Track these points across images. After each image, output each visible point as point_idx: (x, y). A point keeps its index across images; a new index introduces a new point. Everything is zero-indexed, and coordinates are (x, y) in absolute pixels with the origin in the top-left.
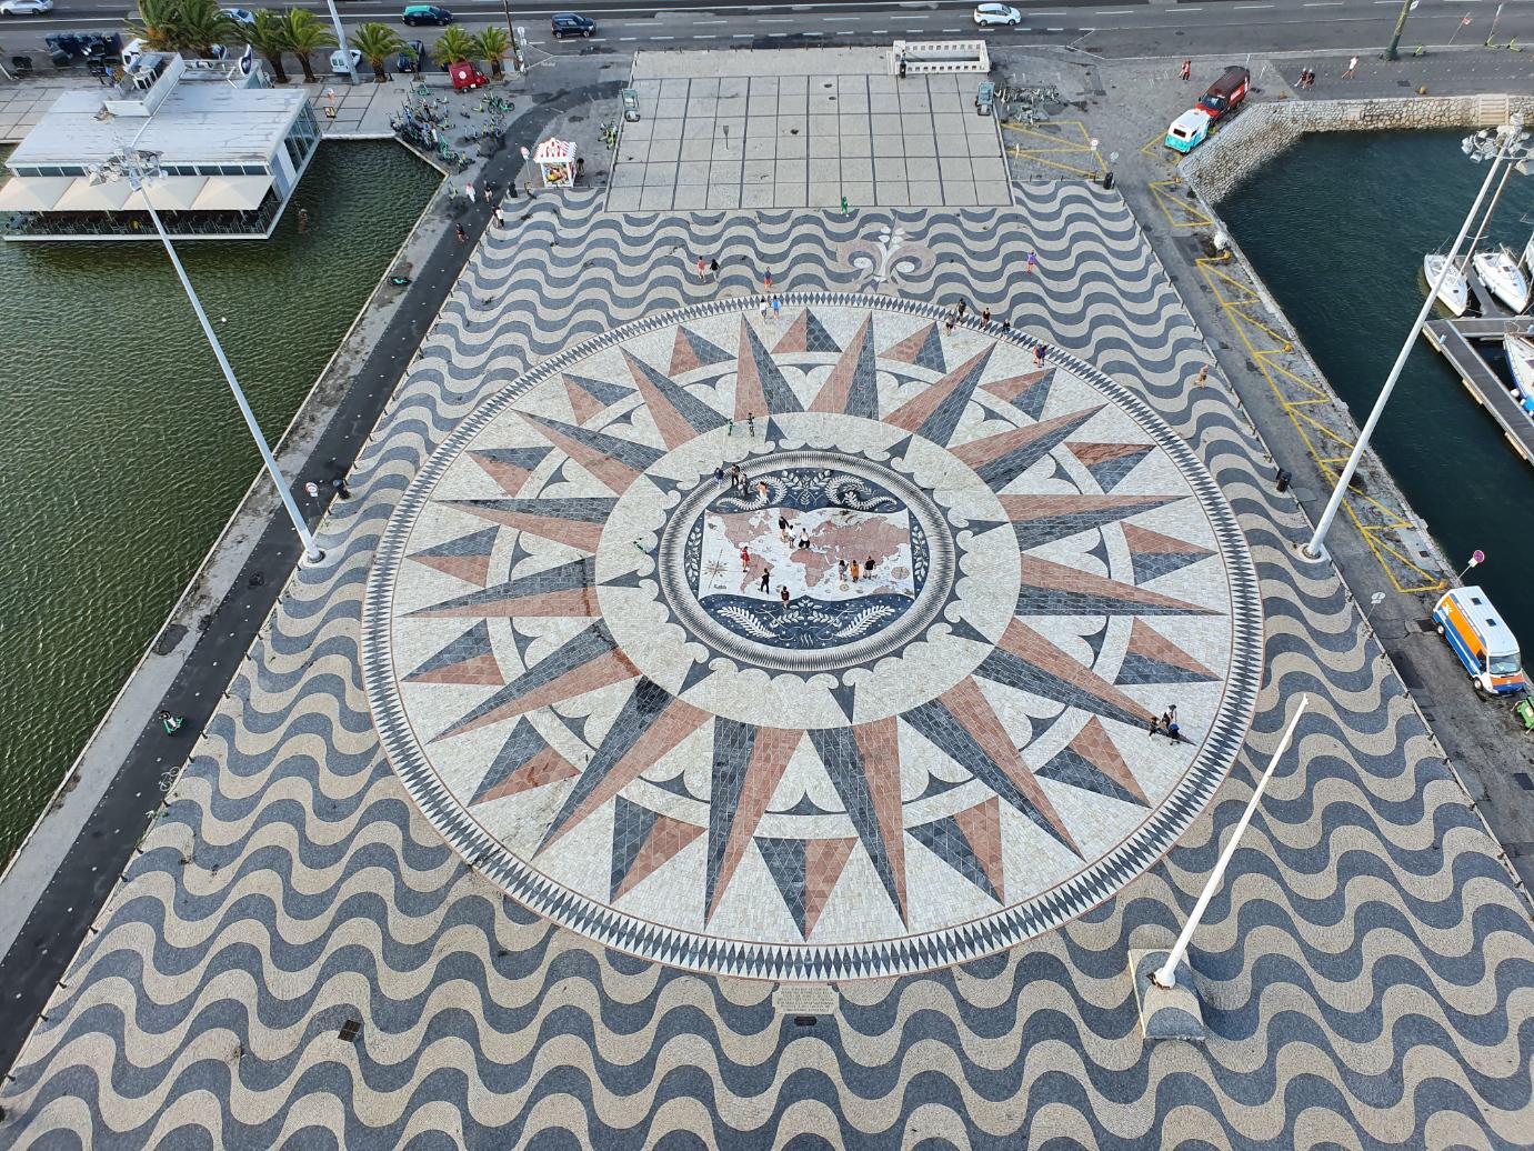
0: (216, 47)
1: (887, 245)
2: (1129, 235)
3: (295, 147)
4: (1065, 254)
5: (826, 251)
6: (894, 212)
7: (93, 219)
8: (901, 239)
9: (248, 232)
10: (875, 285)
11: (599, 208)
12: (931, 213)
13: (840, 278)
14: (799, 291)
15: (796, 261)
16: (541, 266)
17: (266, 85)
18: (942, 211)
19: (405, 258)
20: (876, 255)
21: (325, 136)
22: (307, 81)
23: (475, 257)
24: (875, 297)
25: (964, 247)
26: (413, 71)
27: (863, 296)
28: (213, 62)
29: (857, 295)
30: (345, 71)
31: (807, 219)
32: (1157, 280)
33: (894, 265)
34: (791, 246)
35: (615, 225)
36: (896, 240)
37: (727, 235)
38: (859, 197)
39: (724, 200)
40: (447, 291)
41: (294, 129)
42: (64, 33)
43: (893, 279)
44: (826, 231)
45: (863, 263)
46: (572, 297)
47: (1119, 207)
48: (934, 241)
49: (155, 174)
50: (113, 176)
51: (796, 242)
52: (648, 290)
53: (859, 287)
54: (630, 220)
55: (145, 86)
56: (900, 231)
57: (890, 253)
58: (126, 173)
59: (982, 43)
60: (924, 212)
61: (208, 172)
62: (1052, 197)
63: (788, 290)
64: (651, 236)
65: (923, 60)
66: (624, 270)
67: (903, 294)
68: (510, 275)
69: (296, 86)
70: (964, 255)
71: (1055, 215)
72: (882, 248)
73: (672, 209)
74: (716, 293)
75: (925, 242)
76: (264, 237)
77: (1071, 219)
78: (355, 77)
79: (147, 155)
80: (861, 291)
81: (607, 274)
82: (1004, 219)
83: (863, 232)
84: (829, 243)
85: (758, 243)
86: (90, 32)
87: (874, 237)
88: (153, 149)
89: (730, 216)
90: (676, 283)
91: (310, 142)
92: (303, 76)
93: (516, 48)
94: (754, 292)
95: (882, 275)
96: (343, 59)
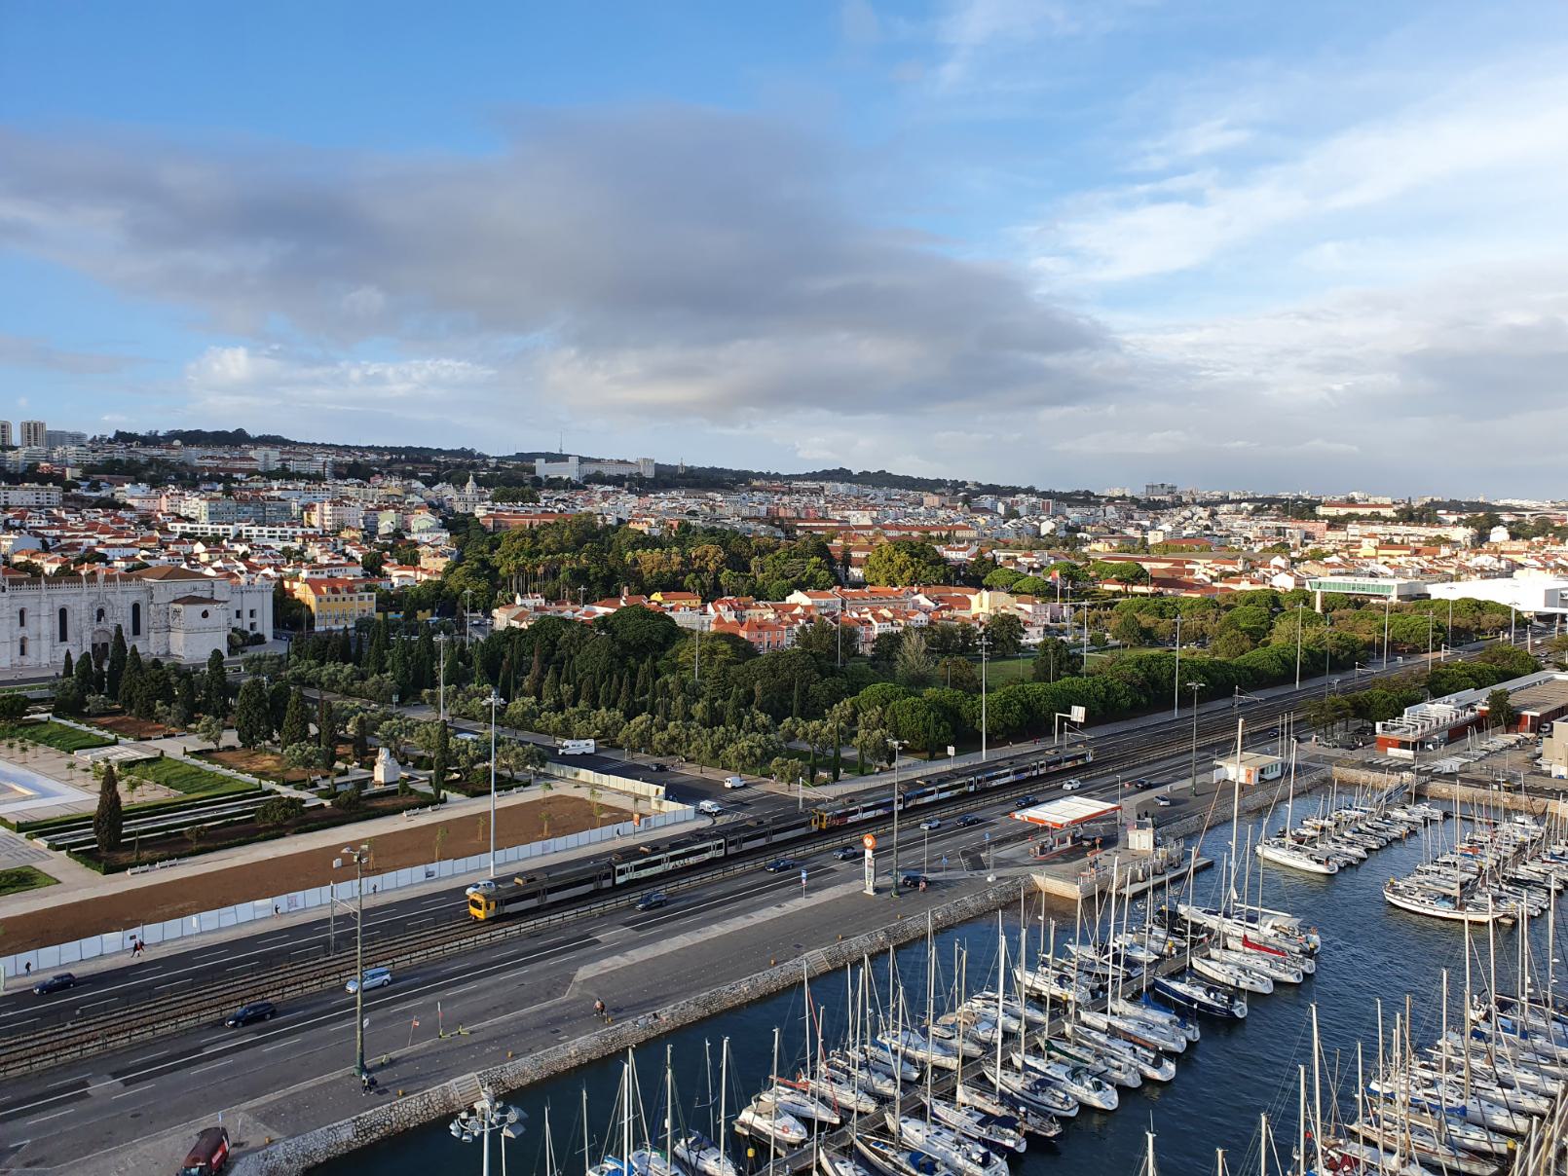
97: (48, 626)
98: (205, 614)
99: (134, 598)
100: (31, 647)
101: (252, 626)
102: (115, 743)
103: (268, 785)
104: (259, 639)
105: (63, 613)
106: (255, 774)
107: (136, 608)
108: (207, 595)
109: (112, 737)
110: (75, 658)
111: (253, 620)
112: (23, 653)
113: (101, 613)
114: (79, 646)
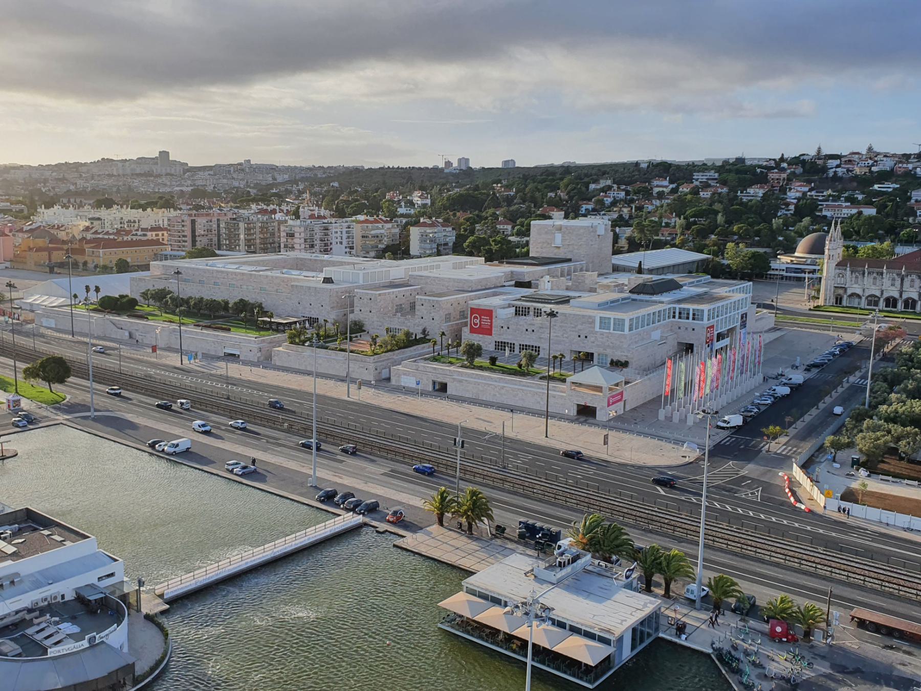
0: (614, 558)
3: (638, 633)
7: (493, 633)
9: (581, 679)
17: (635, 590)
21: (661, 635)
22: (664, 596)
26: (742, 614)
28: (609, 565)
30: (693, 598)
41: (642, 623)
42: (531, 522)
49: (543, 621)
50: (519, 613)
55: (561, 565)
58: (527, 614)
61: (575, 630)
69: (656, 596)
76: (590, 687)
78: (698, 605)
79: (546, 609)
86: (546, 526)
88: (549, 605)
91: (649, 635)
92: (663, 592)
93: (828, 625)
96: (694, 590)
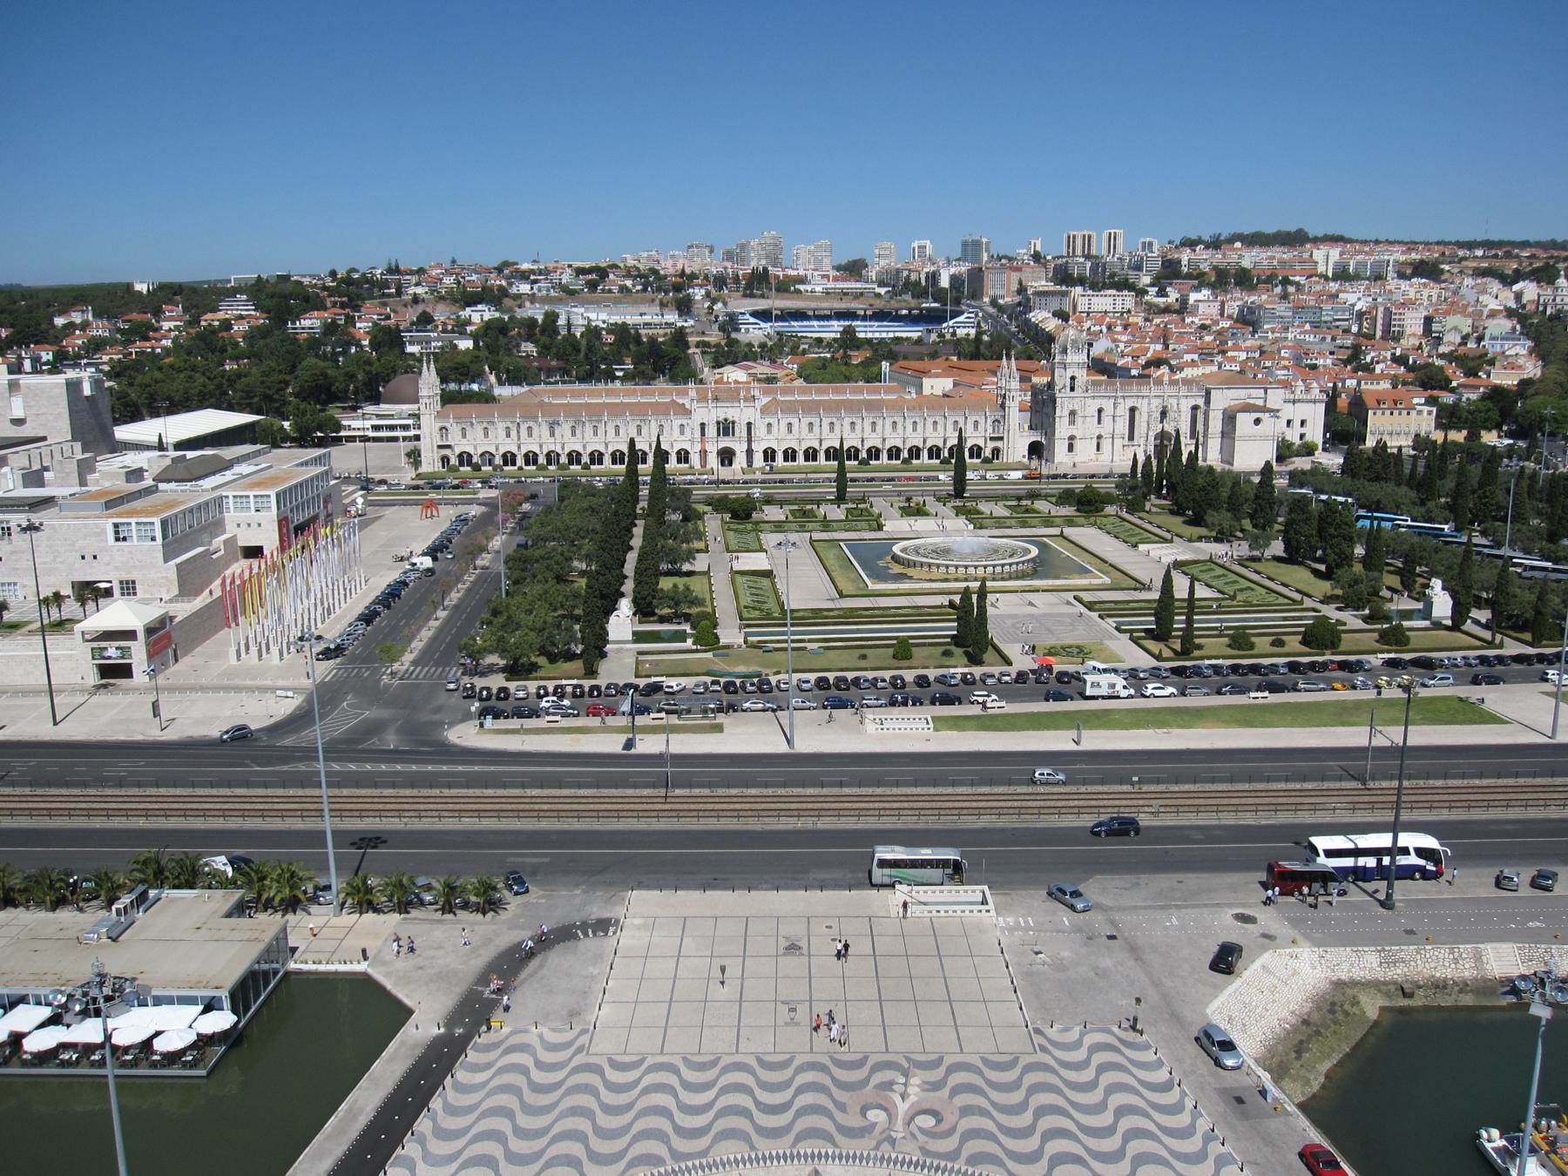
1: (903, 1096)
2: (1166, 1087)
4: (1100, 1108)
5: (835, 1101)
6: (908, 1060)
8: (917, 1089)
10: (893, 1142)
11: (580, 1050)
12: (948, 1061)
13: (849, 1132)
14: (806, 1147)
15: (802, 1112)
16: (508, 1114)
18: (959, 1058)
19: (356, 1101)
20: (889, 1107)
23: (436, 1103)
24: (893, 1156)
25: (988, 1098)
27: (879, 1154)
29: (872, 1154)
31: (813, 1066)
32: (1209, 1137)
33: (912, 1119)
34: (795, 1096)
35: (597, 1069)
36: (911, 1090)
37: (723, 1082)
38: (865, 1041)
39: (717, 1042)
40: (398, 1141)
43: (913, 1135)
44: (834, 1079)
45: (876, 1116)
46: (543, 1151)
47: (1149, 1056)
48: (956, 1091)
51: (800, 1091)
52: (630, 1145)
53: (874, 1143)
54: (614, 1065)
56: (915, 1081)
57: (907, 1105)
59: (986, 888)
60: (941, 1058)
62: (1077, 1045)
63: (794, 1145)
64: (637, 1082)
65: (925, 904)
66: (604, 1121)
67: (926, 1152)
68: (472, 1125)
70: (990, 1109)
71: (1085, 1064)
72: (897, 1099)
73: (662, 1053)
74: (709, 1148)
75: (945, 1093)
77: (1102, 1068)
80: (877, 1148)
81: (584, 1125)
82: (1029, 1068)
83: (878, 1078)
84: (836, 1093)
85: (757, 1091)
87: (888, 1086)
89: (725, 1061)
90: (660, 1135)
94: (752, 1148)
95: (899, 1131)
97: (1122, 426)
98: (1257, 422)
99: (1192, 402)
100: (1106, 444)
101: (1302, 436)
102: (1171, 541)
103: (1308, 603)
104: (1308, 450)
105: (1133, 410)
106: (1298, 591)
107: (1195, 408)
108: (1260, 403)
109: (1168, 536)
110: (1141, 459)
111: (1303, 430)
112: (1098, 449)
113: (1164, 414)
114: (1144, 447)
